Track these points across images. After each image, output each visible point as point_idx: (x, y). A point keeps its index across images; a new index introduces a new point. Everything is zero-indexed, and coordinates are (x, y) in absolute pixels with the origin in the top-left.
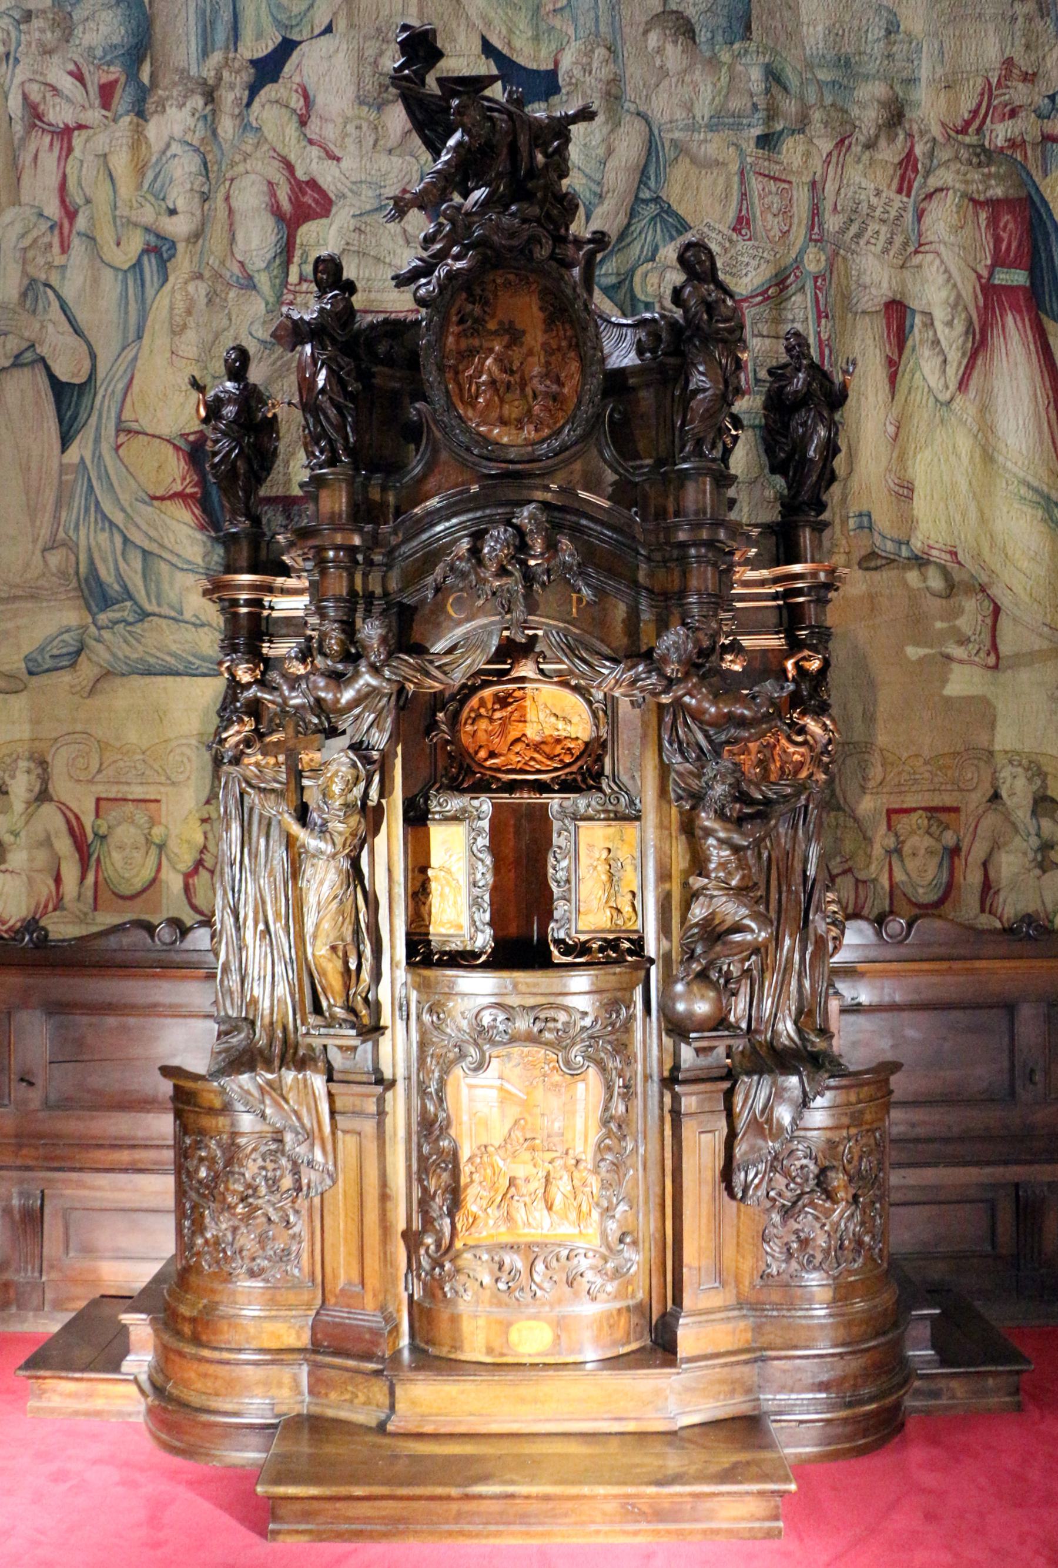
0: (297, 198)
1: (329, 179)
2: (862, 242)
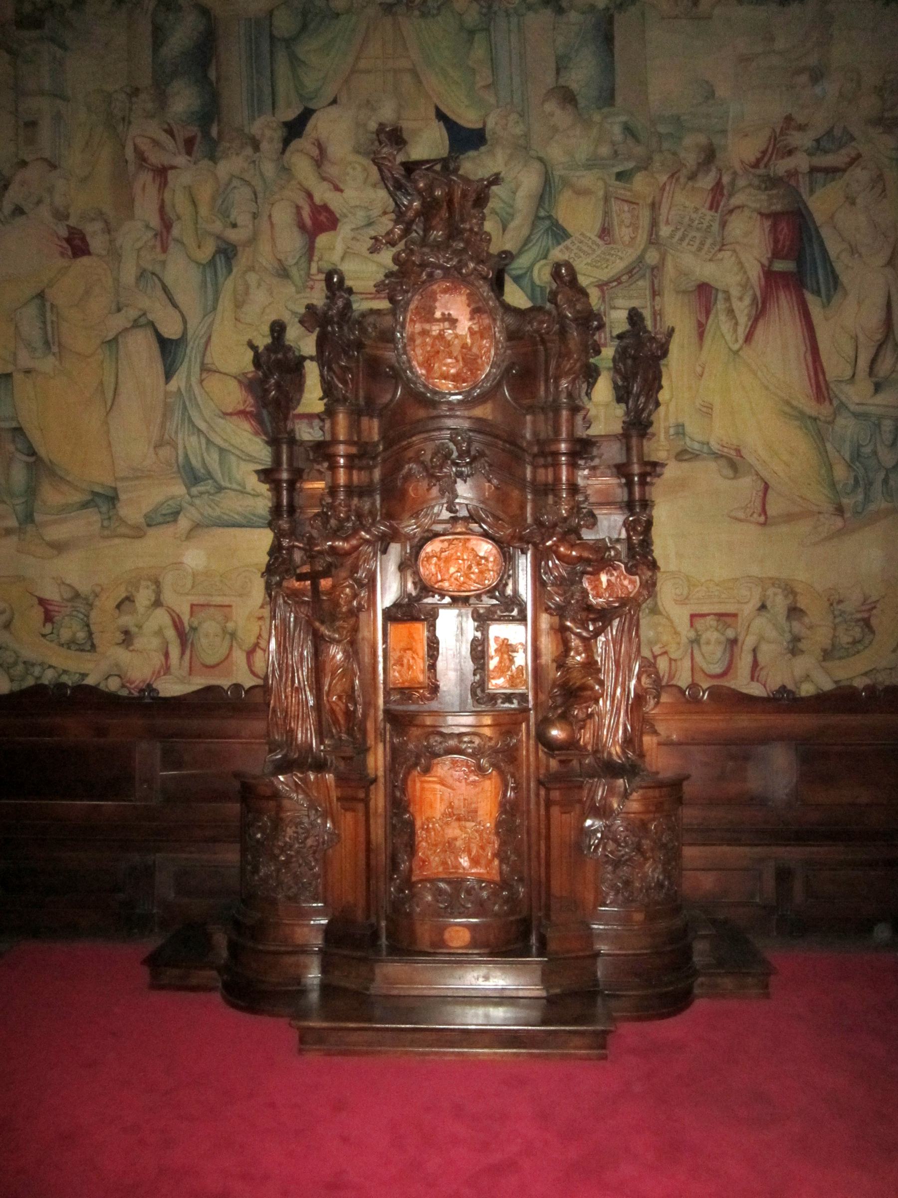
2: (684, 244)
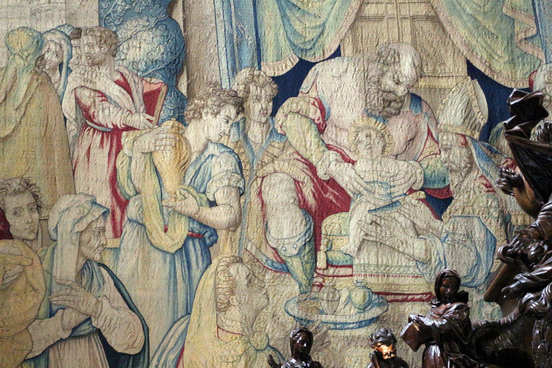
0: (320, 194)
1: (347, 179)
